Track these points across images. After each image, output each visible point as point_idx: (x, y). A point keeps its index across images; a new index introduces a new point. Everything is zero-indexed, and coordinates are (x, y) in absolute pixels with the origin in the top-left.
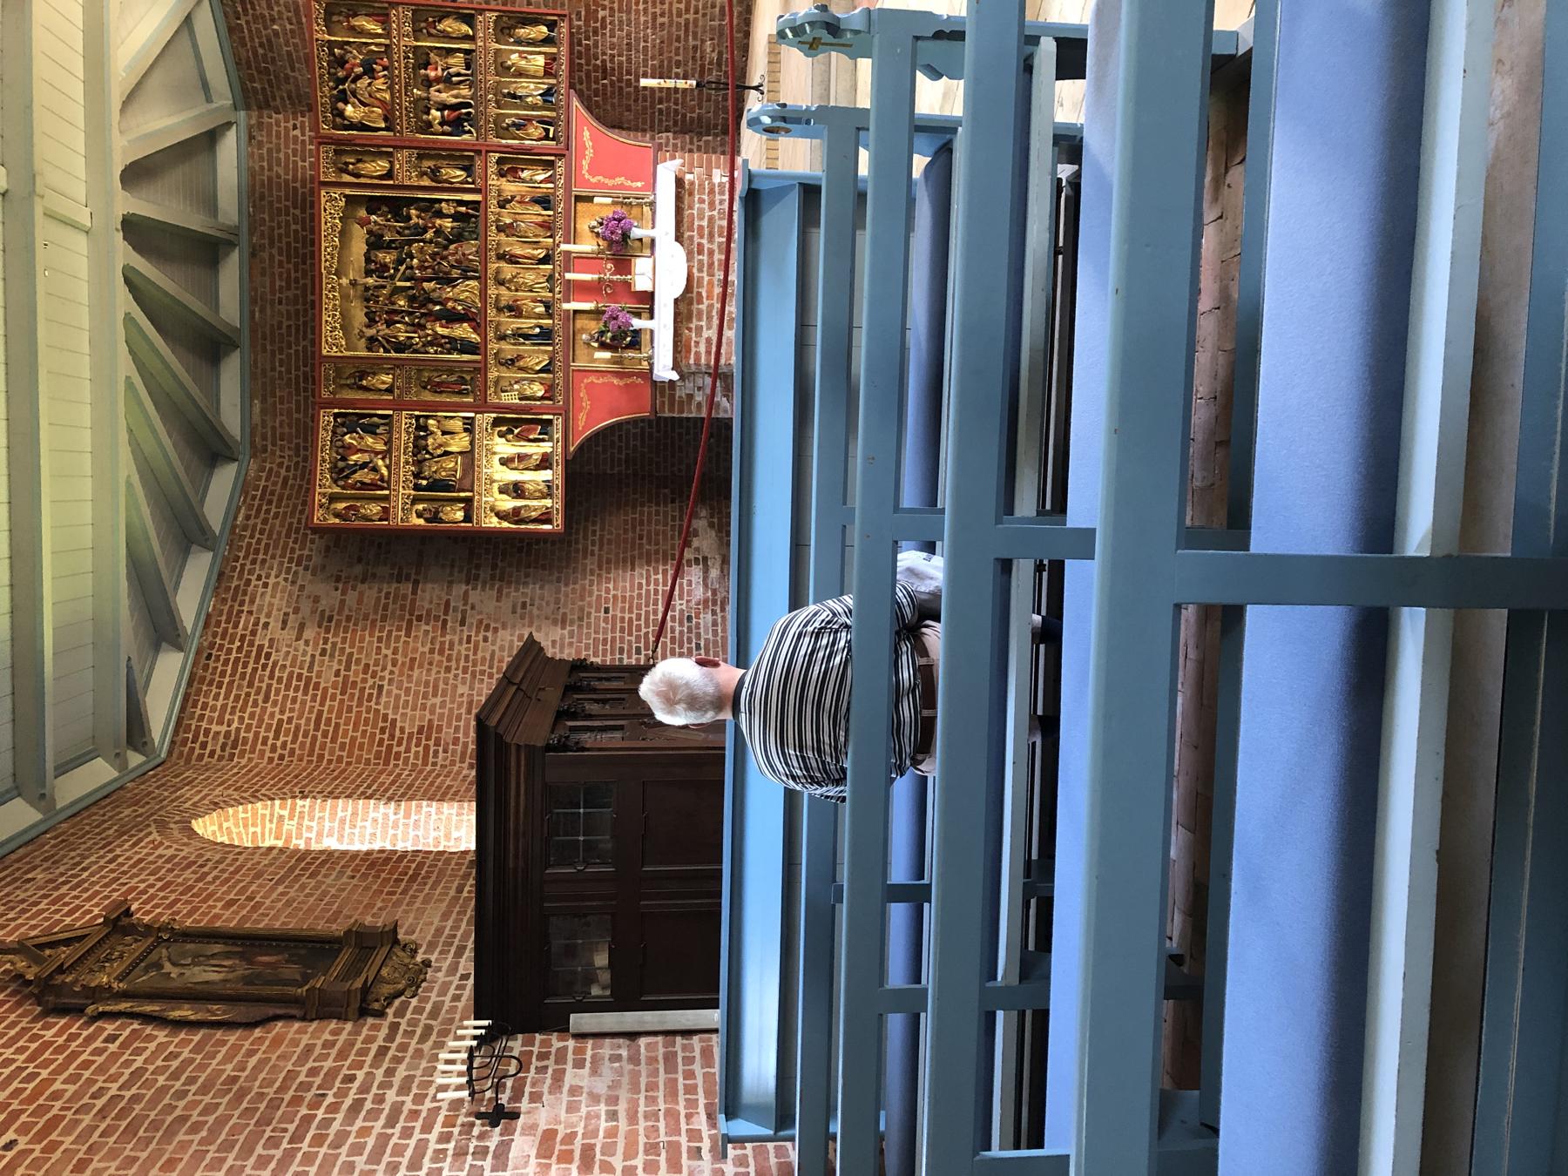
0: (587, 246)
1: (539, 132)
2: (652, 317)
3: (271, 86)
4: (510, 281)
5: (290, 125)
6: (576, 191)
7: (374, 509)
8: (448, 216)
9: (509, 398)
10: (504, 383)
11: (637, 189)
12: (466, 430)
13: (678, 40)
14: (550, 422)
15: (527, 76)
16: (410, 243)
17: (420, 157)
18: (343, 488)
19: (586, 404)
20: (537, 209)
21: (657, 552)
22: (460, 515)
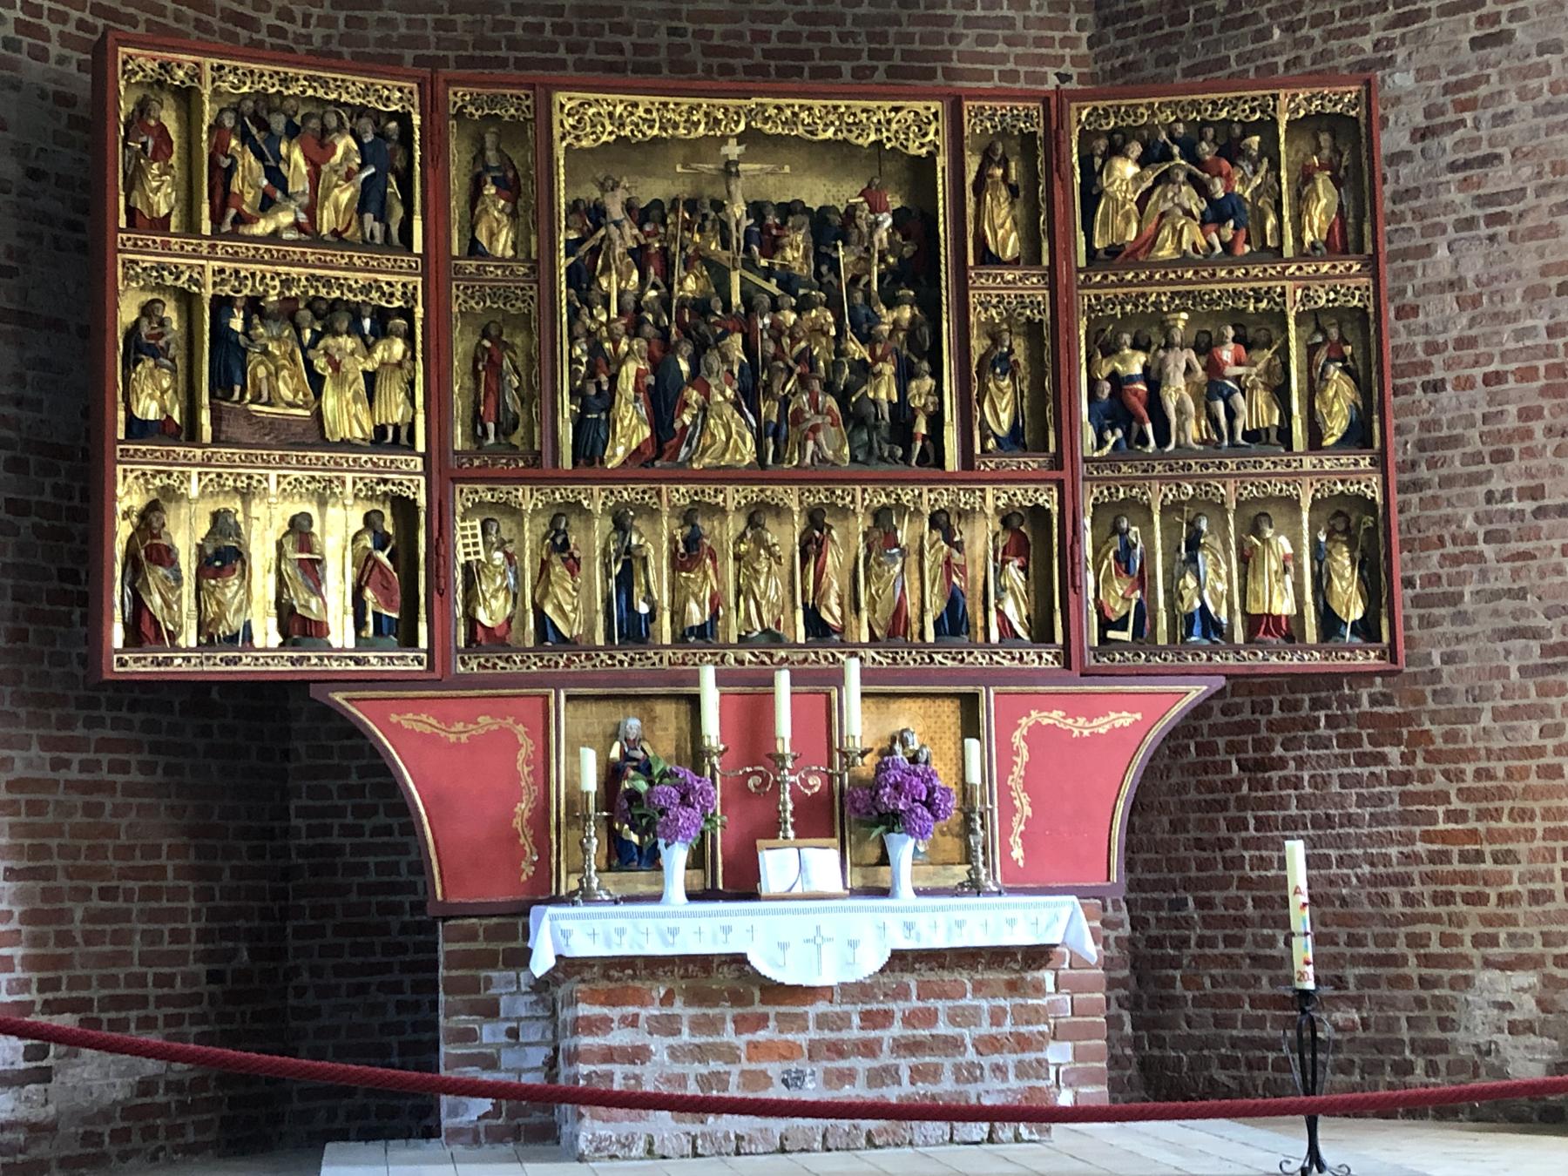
0: (859, 724)
1: (1117, 608)
2: (692, 896)
3: (1148, 28)
4: (760, 542)
5: (1067, 68)
6: (989, 698)
7: (163, 199)
8: (903, 391)
9: (466, 541)
10: (506, 527)
11: (1006, 850)
12: (380, 430)
13: (1354, 940)
14: (411, 641)
15: (1243, 576)
16: (833, 304)
17: (1032, 330)
18: (216, 127)
19: (458, 732)
20: (936, 605)
21: (64, 939)
22: (149, 409)
